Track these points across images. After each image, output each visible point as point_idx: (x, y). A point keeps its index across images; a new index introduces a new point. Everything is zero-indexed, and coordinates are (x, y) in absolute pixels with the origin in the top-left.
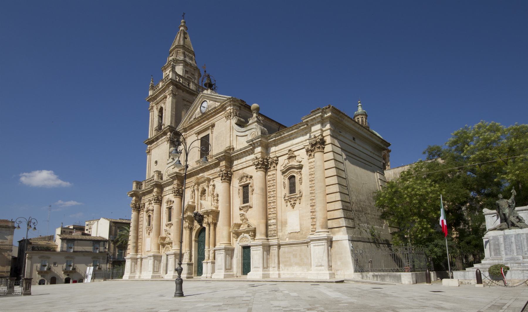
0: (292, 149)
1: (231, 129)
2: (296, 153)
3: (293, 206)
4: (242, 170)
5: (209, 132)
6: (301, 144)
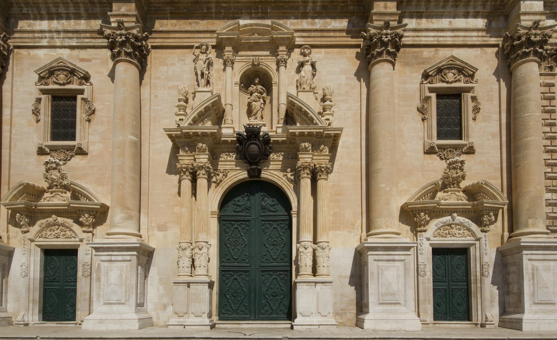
4: (433, 49)
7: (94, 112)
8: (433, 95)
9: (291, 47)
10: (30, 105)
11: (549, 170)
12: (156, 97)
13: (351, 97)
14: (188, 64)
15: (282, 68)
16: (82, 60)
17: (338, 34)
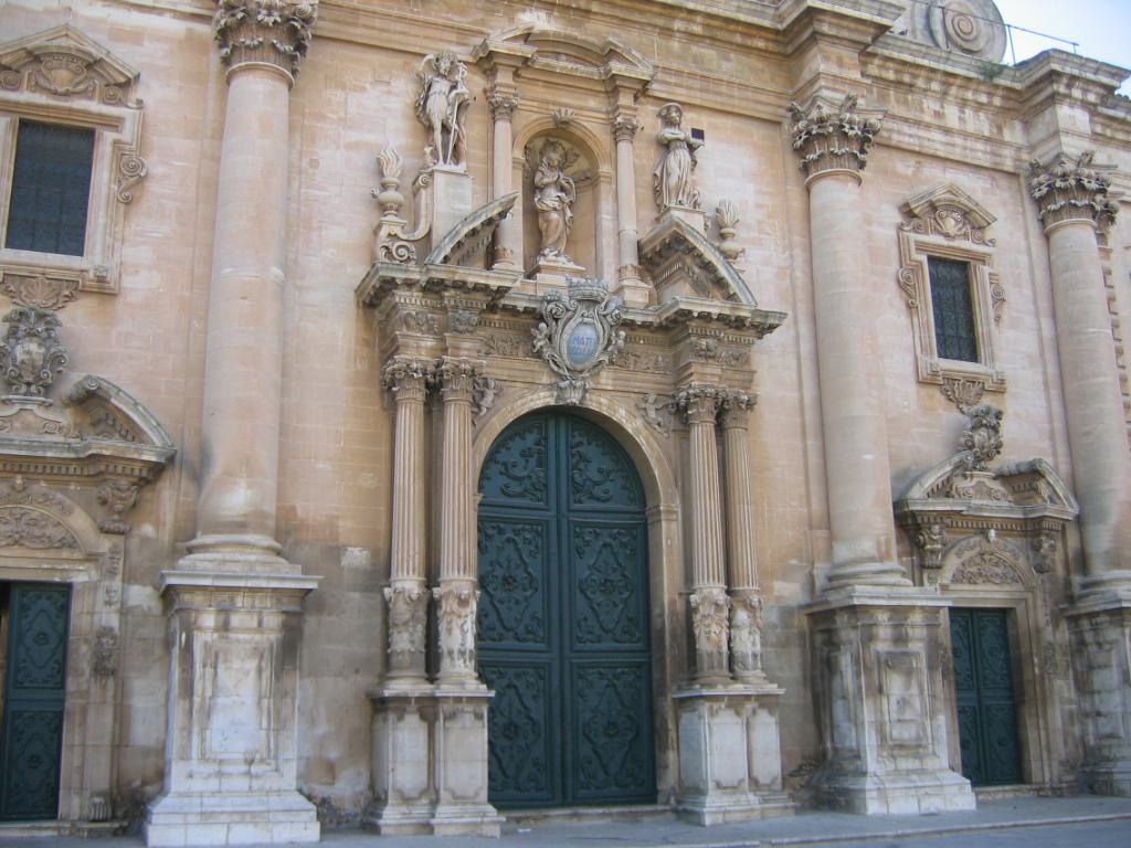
7: (141, 180)
12: (314, 164)
13: (769, 234)
14: (397, 95)
15: (624, 147)
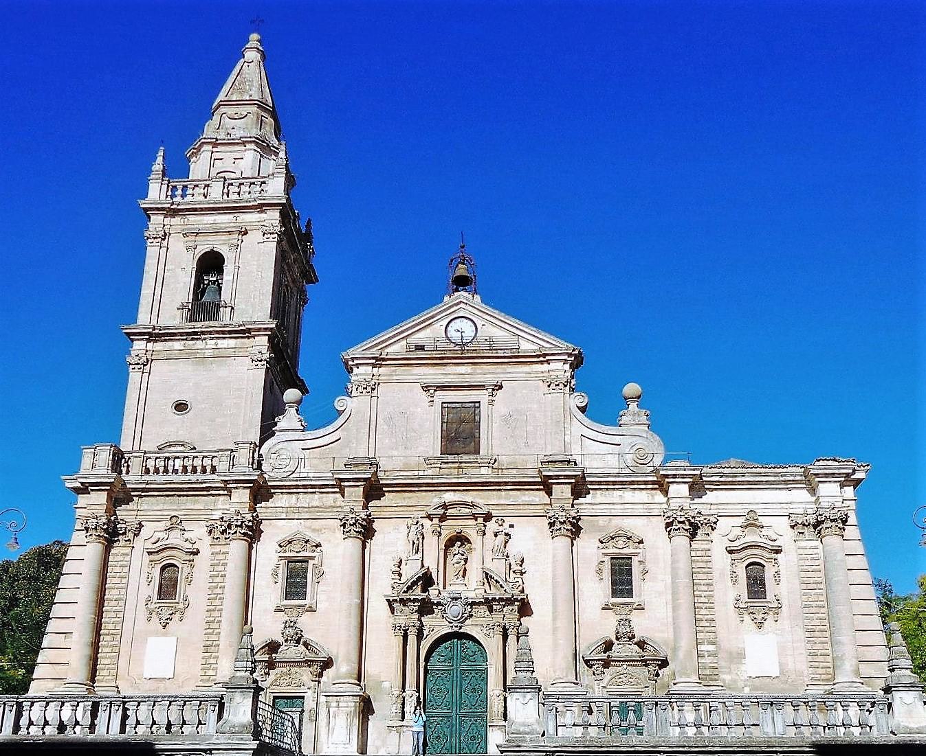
0: (757, 511)
1: (566, 415)
2: (764, 521)
3: (760, 625)
5: (482, 396)
6: (779, 506)
8: (607, 559)
9: (488, 517)
10: (270, 568)
11: (708, 625)
16: (314, 530)
17: (526, 507)
